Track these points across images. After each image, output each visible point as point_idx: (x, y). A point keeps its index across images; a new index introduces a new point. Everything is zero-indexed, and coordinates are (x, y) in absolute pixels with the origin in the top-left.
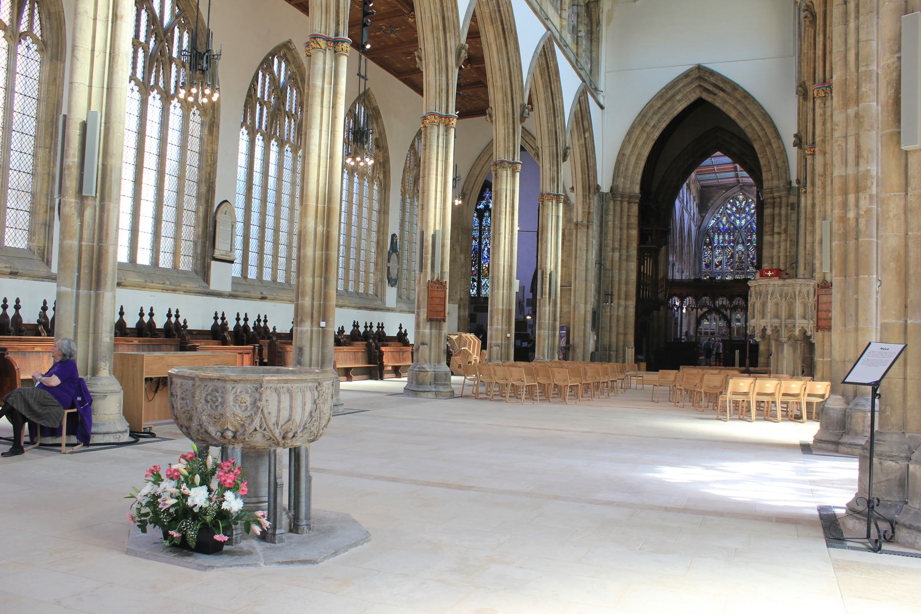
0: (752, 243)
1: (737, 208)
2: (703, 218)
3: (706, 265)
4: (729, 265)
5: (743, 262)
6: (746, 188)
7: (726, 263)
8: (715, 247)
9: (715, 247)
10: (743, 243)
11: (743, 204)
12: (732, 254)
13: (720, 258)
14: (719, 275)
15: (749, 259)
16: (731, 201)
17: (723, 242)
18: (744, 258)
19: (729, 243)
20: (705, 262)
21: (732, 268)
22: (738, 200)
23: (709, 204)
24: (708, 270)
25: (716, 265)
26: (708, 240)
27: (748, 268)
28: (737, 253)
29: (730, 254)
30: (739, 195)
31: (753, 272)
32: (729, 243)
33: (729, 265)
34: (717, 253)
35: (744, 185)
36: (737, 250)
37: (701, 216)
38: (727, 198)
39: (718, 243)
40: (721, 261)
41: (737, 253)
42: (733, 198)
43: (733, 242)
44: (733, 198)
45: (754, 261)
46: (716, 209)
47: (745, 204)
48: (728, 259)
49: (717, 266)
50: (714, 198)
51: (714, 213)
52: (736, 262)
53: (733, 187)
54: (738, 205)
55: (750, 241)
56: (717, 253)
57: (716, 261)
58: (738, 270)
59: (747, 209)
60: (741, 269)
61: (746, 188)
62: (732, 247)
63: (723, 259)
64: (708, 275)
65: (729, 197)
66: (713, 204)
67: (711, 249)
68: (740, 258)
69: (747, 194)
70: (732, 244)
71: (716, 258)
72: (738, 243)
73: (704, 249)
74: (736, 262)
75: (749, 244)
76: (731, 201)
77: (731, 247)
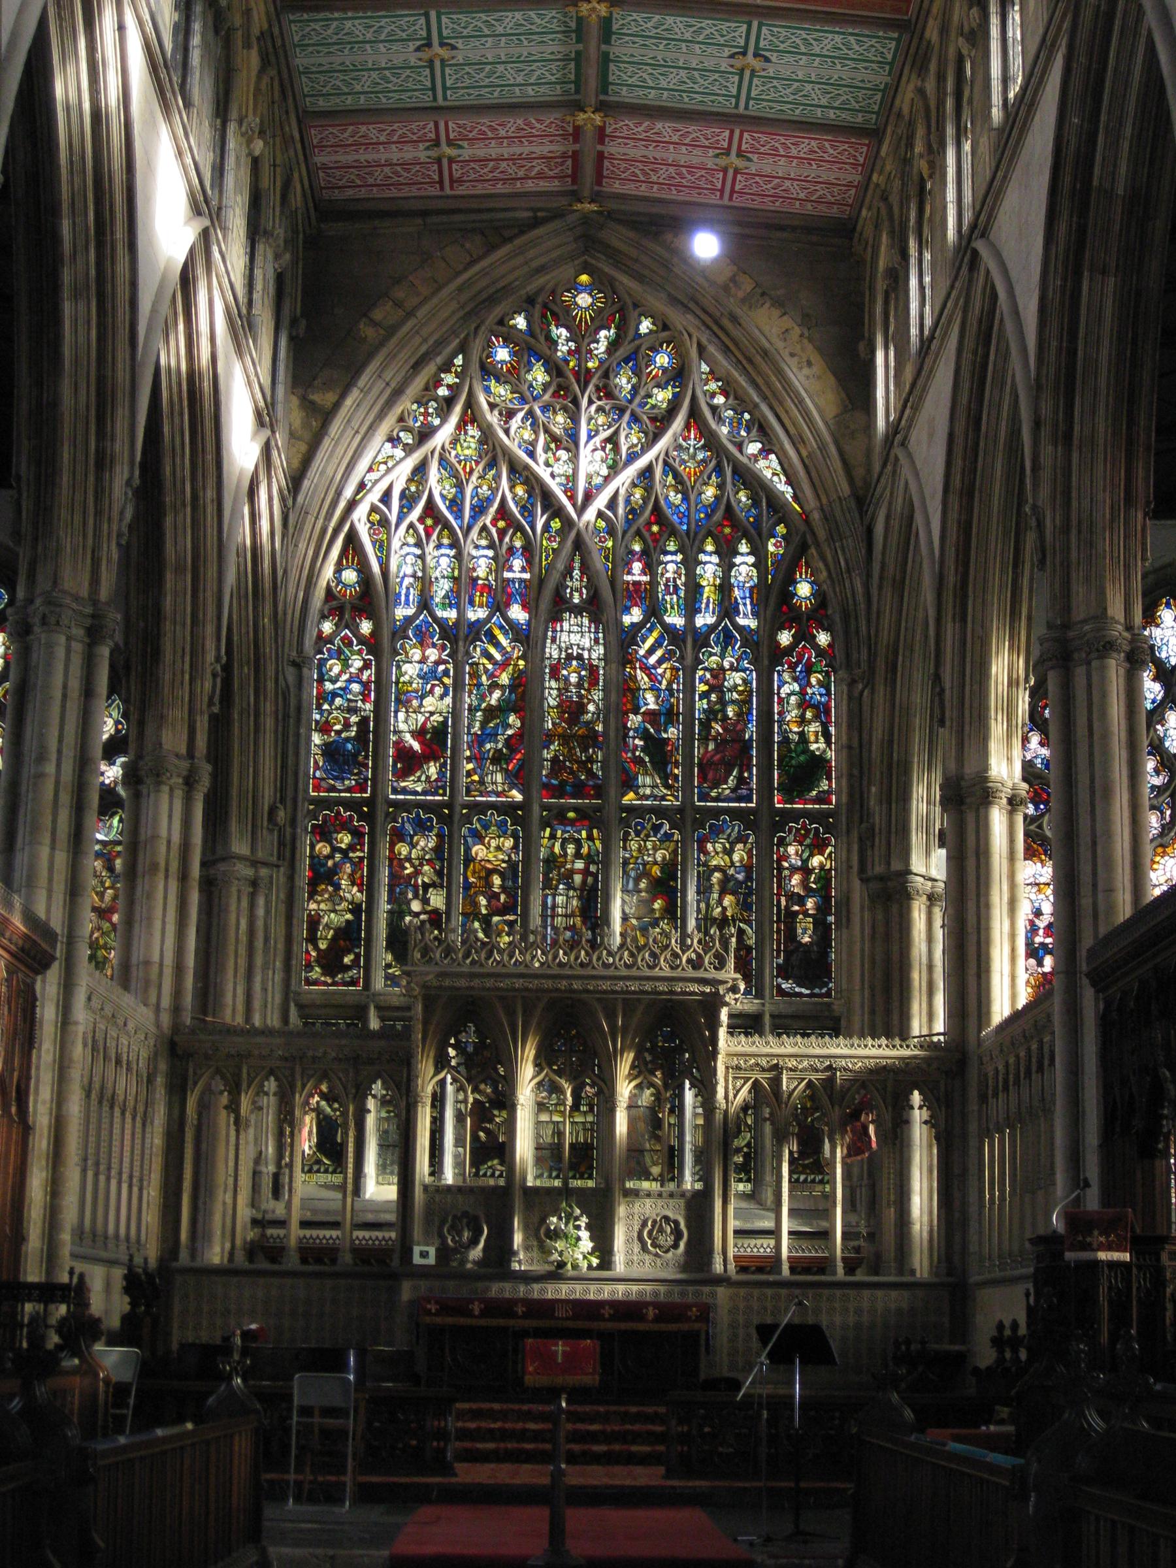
0: (654, 612)
1: (555, 369)
2: (326, 416)
3: (330, 751)
4: (498, 758)
5: (590, 739)
6: (617, 237)
7: (479, 740)
8: (400, 632)
9: (400, 632)
10: (594, 608)
11: (601, 348)
12: (519, 681)
13: (436, 705)
14: (422, 827)
15: (634, 720)
16: (520, 322)
17: (453, 599)
18: (605, 713)
19: (499, 606)
20: (325, 728)
21: (517, 778)
22: (564, 316)
23: (368, 332)
24: (344, 787)
25: (404, 753)
26: (350, 576)
27: (629, 784)
28: (555, 674)
29: (504, 679)
30: (576, 288)
31: (660, 812)
32: (499, 606)
33: (498, 758)
34: (411, 670)
35: (610, 215)
36: (552, 651)
37: (309, 407)
38: (492, 300)
39: (425, 604)
40: (440, 732)
41: (555, 674)
42: (531, 301)
43: (530, 596)
44: (528, 304)
45: (672, 733)
46: (417, 366)
47: (613, 346)
48: (491, 713)
49: (409, 762)
50: (399, 293)
51: (398, 393)
52: (549, 737)
53: (536, 223)
54: (563, 348)
55: (636, 593)
56: (411, 670)
57: (404, 724)
58: (559, 791)
59: (624, 382)
60: (579, 790)
61: (617, 237)
62: (519, 634)
63: (455, 711)
64: (345, 826)
65: (506, 290)
66: (392, 330)
67: (372, 644)
68: (572, 710)
69: (625, 280)
70: (517, 613)
71: (403, 701)
72: (560, 606)
73: (321, 640)
74: (549, 737)
75: (635, 616)
76: (520, 322)
77: (513, 628)
